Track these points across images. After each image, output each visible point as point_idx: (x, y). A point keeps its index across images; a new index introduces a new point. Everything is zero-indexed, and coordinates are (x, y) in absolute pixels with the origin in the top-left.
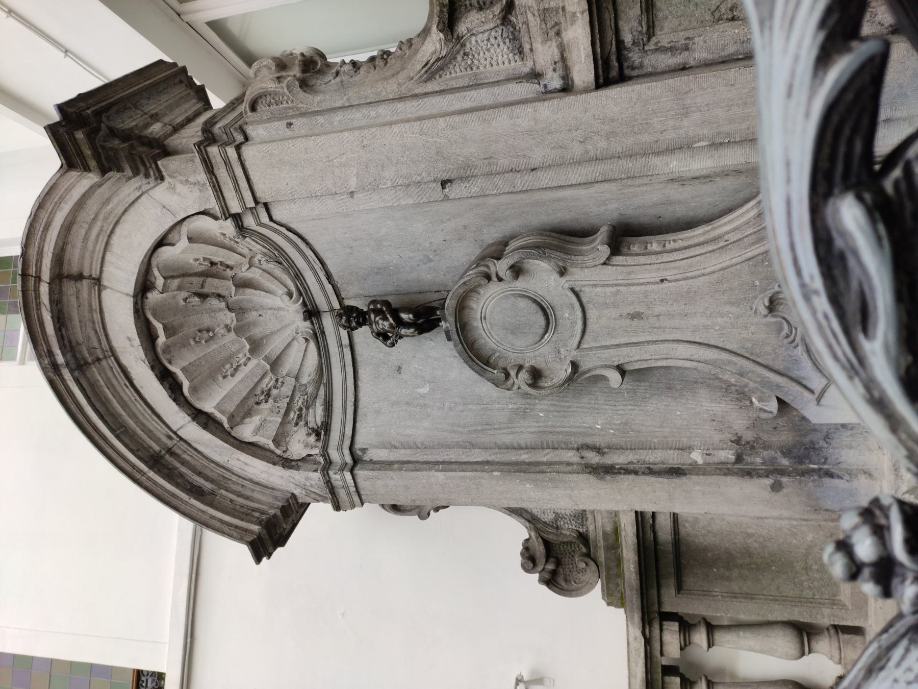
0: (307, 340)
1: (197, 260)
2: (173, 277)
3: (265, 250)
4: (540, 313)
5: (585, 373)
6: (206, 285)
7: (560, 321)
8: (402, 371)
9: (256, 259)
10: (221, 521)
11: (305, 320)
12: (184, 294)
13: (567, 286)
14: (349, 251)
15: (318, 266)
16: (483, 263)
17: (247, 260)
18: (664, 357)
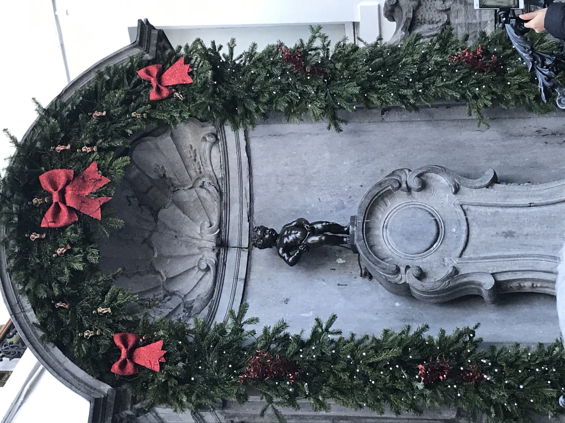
0: (208, 269)
1: (157, 166)
2: (138, 167)
3: (212, 174)
4: (434, 222)
5: (465, 276)
6: (150, 191)
7: (448, 234)
8: (289, 302)
9: (200, 183)
10: (73, 375)
11: (214, 250)
12: (130, 193)
13: (458, 202)
14: (279, 188)
15: (246, 201)
16: (398, 172)
17: (193, 181)
18: (530, 269)
